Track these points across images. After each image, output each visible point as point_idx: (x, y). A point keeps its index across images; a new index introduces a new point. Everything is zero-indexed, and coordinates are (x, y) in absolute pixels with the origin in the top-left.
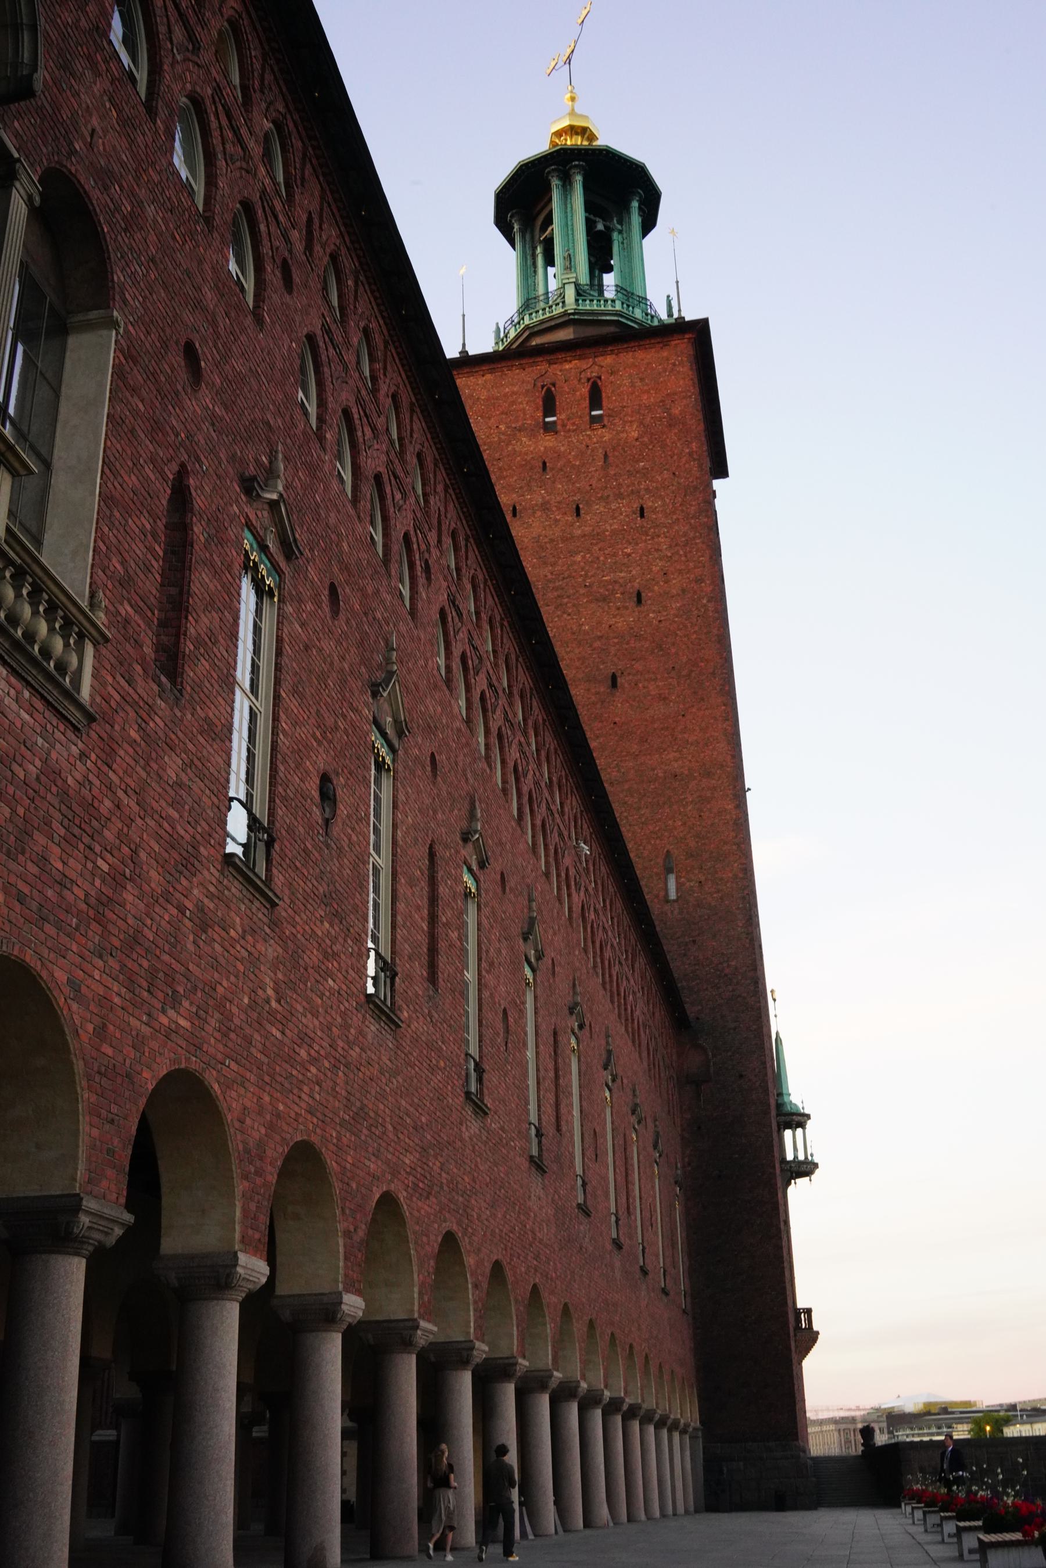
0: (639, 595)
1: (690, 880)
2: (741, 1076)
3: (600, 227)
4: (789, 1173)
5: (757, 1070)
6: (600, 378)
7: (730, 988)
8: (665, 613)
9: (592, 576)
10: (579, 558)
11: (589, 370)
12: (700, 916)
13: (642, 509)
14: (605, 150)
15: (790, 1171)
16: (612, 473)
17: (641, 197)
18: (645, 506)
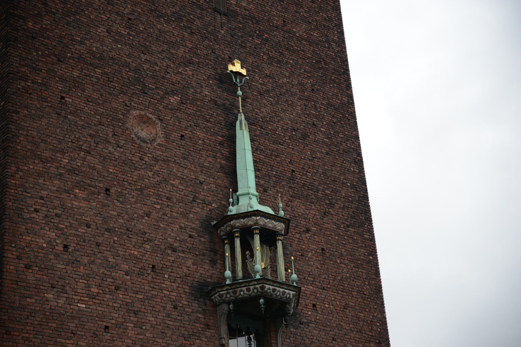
15: (224, 302)
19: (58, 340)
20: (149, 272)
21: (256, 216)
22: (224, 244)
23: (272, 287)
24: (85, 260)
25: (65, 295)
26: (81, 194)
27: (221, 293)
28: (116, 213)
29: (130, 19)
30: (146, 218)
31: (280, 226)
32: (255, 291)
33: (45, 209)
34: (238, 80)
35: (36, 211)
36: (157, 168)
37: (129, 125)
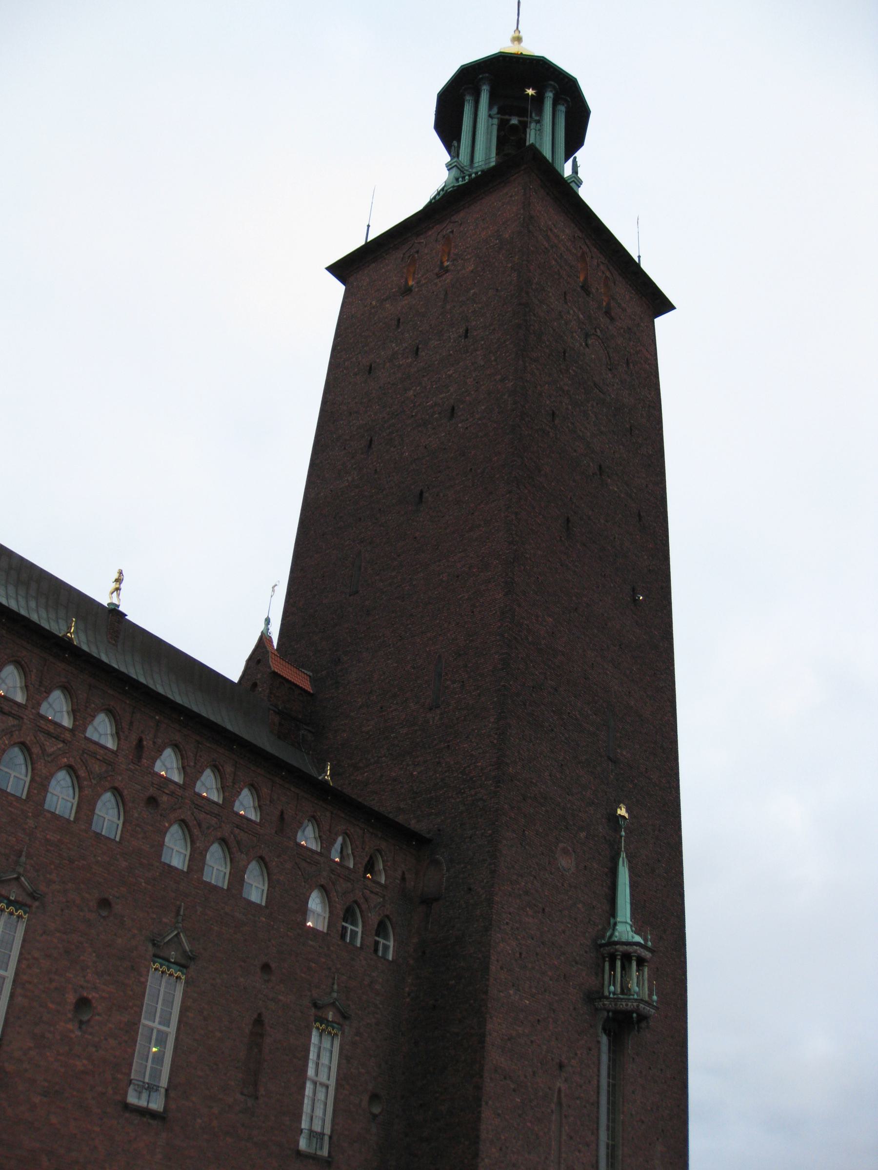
0: (453, 409)
1: (454, 682)
2: (470, 889)
3: (514, 121)
4: (605, 1014)
5: (485, 881)
6: (452, 232)
7: (473, 792)
8: (471, 419)
9: (419, 405)
10: (411, 393)
11: (445, 229)
12: (457, 719)
13: (467, 331)
14: (501, 56)
16: (448, 307)
17: (554, 87)
18: (469, 327)
19: (515, 1026)
20: (562, 979)
21: (636, 946)
22: (604, 961)
23: (643, 1006)
24: (530, 966)
25: (519, 993)
26: (530, 911)
27: (605, 1002)
28: (547, 929)
29: (562, 765)
30: (563, 935)
31: (647, 955)
32: (632, 1007)
33: (511, 923)
34: (623, 823)
35: (507, 923)
36: (570, 893)
37: (556, 856)
